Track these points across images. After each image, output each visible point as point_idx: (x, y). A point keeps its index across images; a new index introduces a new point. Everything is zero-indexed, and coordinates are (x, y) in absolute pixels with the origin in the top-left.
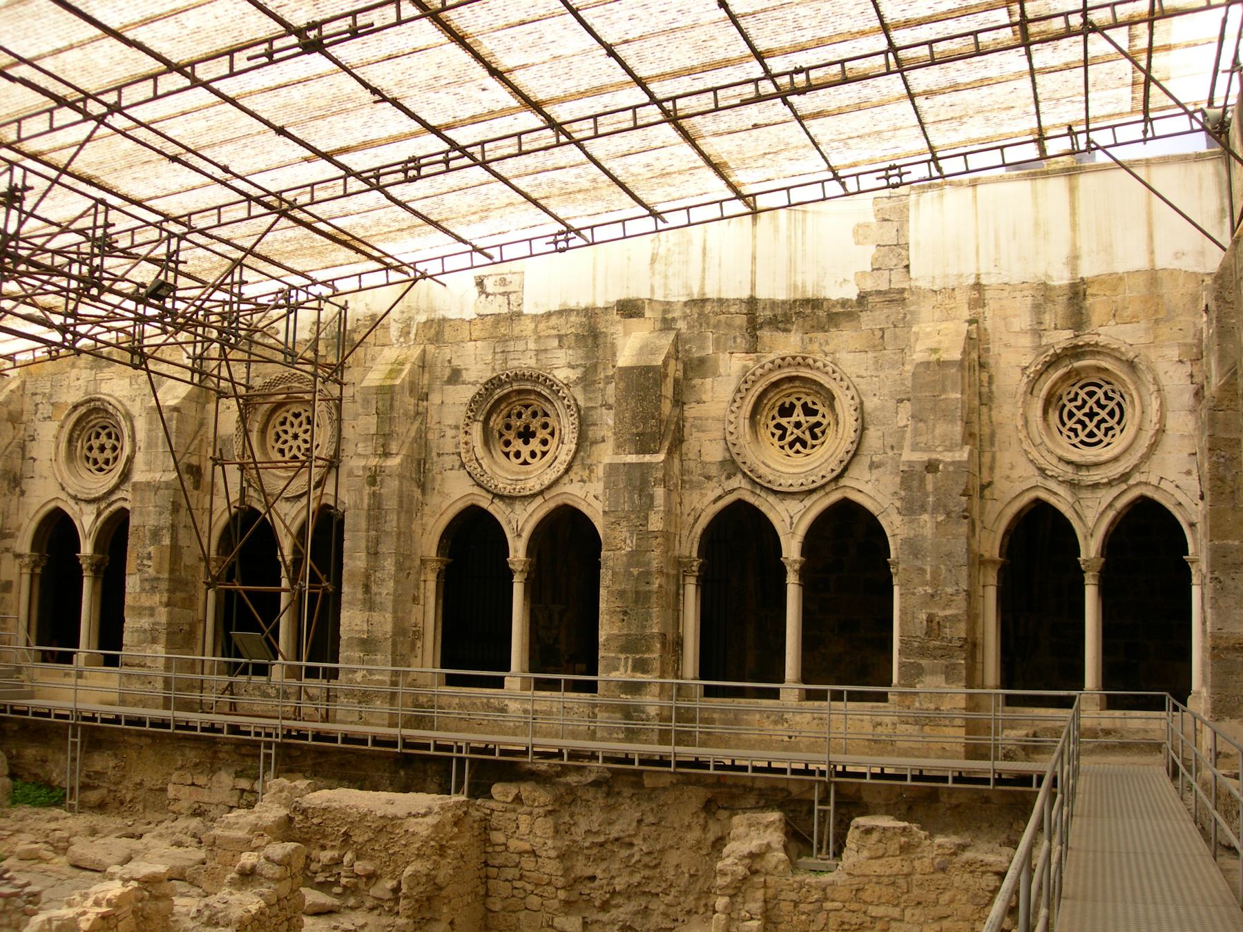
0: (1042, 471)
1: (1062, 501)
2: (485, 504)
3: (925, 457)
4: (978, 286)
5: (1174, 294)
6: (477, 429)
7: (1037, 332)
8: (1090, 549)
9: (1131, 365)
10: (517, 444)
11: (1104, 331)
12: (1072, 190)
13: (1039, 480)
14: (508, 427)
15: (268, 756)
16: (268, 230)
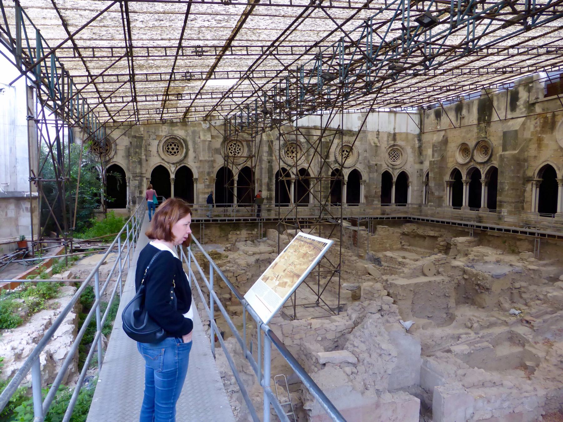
0: (388, 166)
1: (391, 171)
2: (286, 167)
3: (375, 163)
4: (378, 131)
5: (410, 137)
6: (283, 151)
7: (388, 141)
8: (395, 179)
9: (403, 149)
10: (290, 155)
11: (399, 142)
12: (395, 116)
13: (387, 167)
14: (288, 150)
15: (261, 225)
16: (110, 67)
